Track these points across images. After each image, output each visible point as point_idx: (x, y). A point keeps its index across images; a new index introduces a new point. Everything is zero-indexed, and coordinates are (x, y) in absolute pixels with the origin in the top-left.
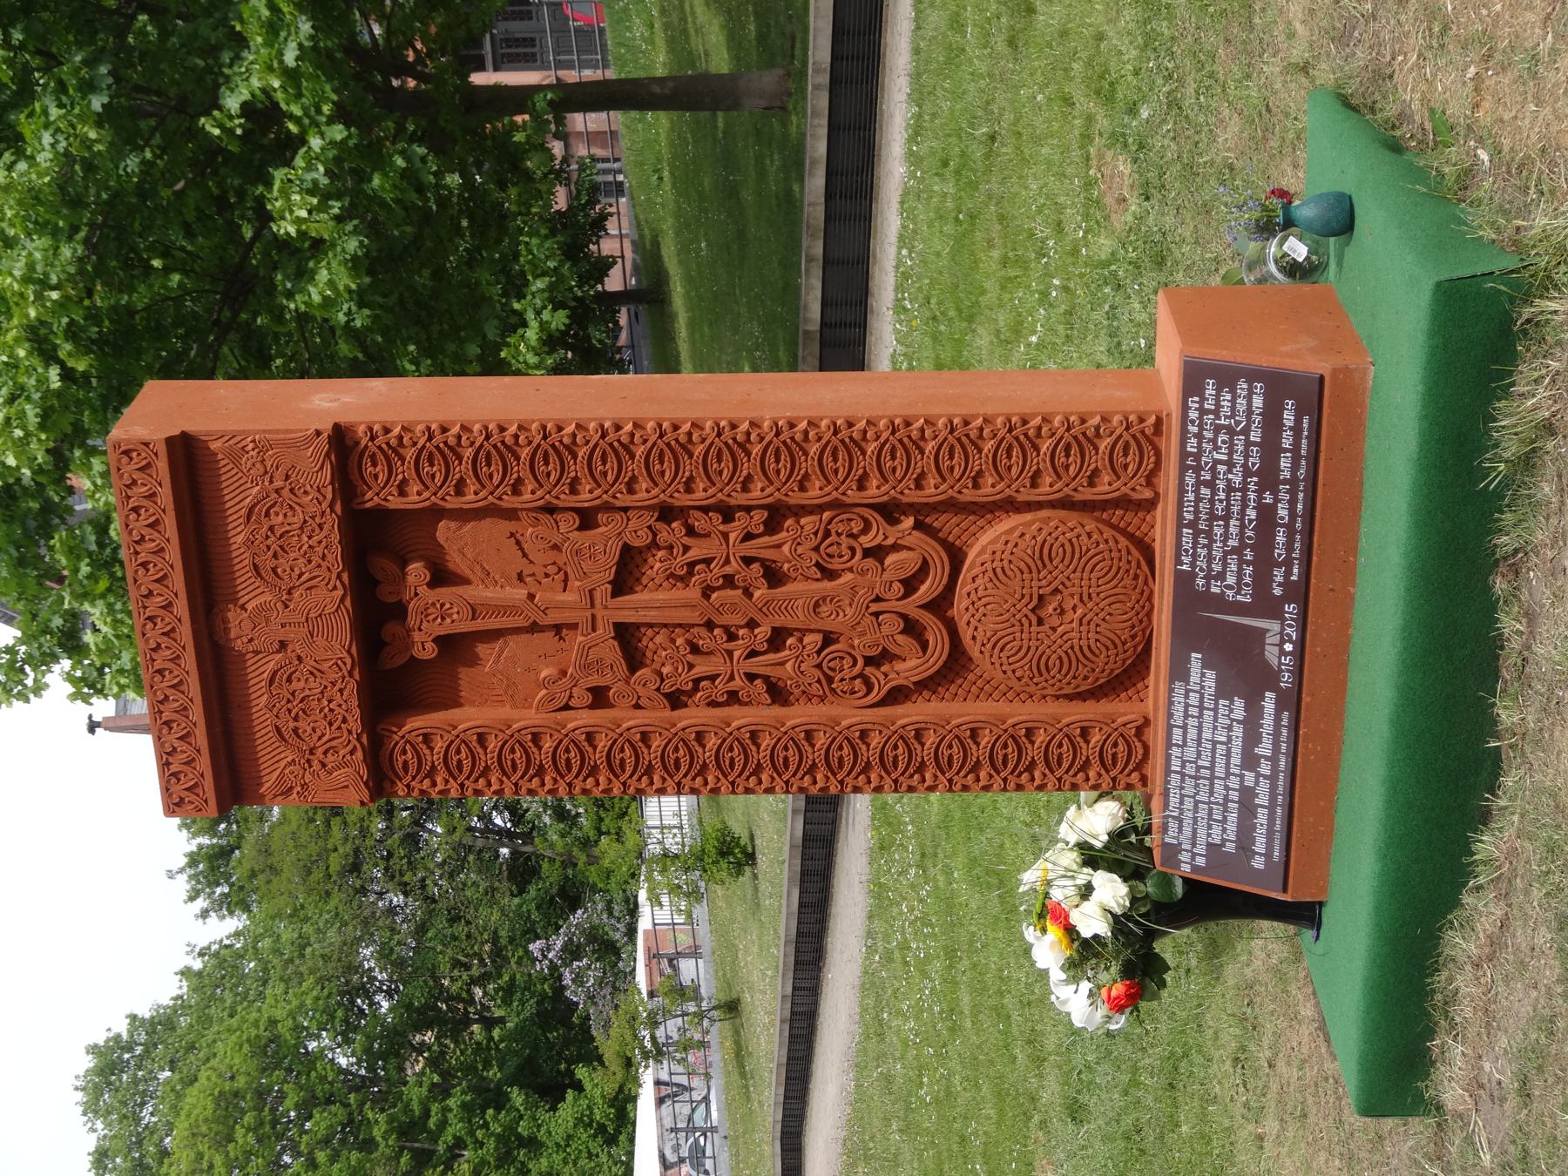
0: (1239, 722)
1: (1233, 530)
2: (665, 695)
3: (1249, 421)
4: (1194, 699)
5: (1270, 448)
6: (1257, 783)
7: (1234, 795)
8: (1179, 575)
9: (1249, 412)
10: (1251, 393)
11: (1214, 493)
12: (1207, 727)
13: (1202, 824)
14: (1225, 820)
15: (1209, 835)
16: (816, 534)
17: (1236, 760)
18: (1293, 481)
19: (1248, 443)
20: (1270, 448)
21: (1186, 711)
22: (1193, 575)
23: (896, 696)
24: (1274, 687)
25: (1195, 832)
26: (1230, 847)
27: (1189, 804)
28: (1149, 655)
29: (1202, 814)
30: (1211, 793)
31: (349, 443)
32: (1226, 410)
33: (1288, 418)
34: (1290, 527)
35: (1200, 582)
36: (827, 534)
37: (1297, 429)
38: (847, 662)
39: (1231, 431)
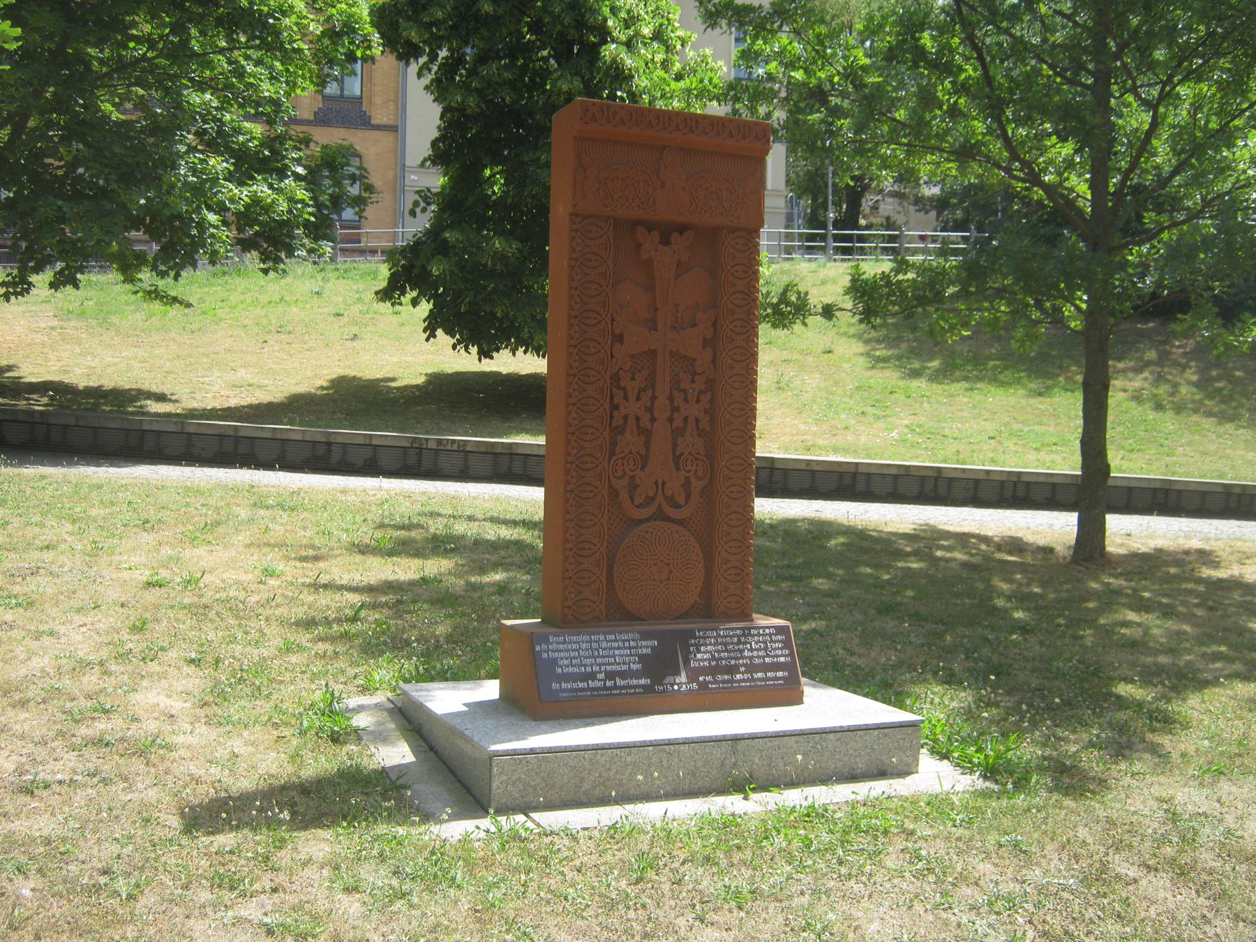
1: (722, 654)
4: (632, 643)
5: (766, 668)
7: (589, 669)
9: (777, 656)
10: (785, 656)
11: (736, 644)
13: (567, 654)
14: (573, 666)
17: (608, 668)
18: (753, 680)
20: (766, 668)
24: (653, 684)
25: (561, 651)
26: (559, 670)
29: (572, 654)
31: (753, 234)
32: (774, 646)
33: (780, 674)
34: (732, 681)
35: (693, 641)
36: (697, 459)
37: (776, 678)
38: (633, 468)
39: (766, 649)
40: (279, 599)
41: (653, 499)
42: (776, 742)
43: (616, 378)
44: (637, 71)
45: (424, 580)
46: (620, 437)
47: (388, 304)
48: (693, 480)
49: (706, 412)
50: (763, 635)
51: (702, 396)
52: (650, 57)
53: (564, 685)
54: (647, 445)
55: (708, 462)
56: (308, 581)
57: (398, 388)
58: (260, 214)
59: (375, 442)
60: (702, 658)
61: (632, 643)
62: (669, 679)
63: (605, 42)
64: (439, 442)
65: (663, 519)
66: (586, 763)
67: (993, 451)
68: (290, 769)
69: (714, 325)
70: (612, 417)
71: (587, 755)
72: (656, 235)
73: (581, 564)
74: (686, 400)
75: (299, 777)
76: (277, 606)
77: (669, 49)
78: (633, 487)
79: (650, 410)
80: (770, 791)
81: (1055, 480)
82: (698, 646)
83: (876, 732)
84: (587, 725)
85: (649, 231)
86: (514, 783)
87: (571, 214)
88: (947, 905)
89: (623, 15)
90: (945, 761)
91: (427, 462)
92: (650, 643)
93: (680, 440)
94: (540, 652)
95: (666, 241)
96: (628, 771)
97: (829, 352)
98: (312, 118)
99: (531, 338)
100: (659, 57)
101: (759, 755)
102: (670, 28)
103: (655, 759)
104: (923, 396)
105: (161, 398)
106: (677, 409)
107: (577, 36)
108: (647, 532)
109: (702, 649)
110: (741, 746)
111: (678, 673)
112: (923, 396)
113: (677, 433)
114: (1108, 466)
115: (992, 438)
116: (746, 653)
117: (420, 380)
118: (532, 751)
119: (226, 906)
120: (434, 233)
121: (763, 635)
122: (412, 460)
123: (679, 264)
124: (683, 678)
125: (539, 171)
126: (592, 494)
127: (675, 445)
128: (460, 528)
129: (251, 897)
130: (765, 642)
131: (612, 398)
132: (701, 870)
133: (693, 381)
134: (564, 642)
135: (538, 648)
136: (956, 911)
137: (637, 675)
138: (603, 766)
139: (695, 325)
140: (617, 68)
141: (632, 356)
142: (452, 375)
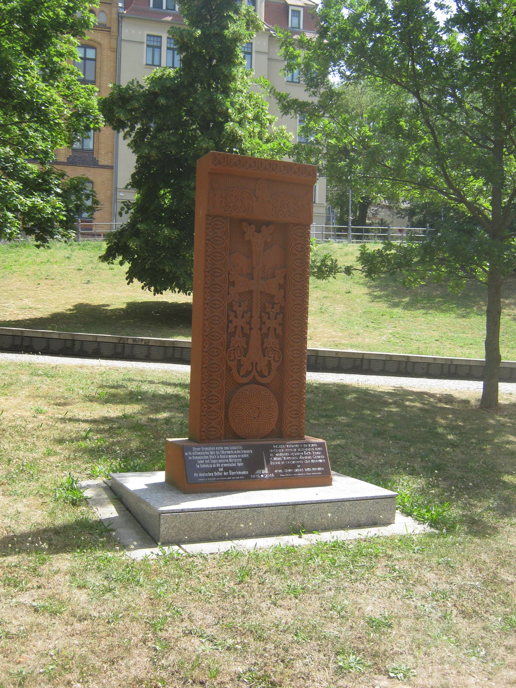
0: (237, 465)
2: (232, 302)
4: (238, 452)
5: (312, 465)
6: (220, 472)
7: (214, 466)
8: (272, 445)
9: (318, 459)
11: (295, 452)
14: (206, 464)
15: (199, 460)
16: (275, 347)
18: (305, 472)
19: (310, 460)
20: (312, 465)
21: (235, 450)
22: (273, 449)
25: (199, 456)
26: (198, 466)
27: (207, 453)
28: (237, 438)
29: (205, 457)
30: (213, 459)
33: (319, 469)
34: (293, 473)
35: (272, 451)
36: (275, 351)
39: (312, 455)
40: (44, 426)
41: (250, 372)
42: (317, 506)
43: (230, 305)
44: (245, 138)
45: (125, 416)
46: (232, 338)
47: (106, 263)
48: (272, 362)
49: (280, 324)
51: (278, 316)
52: (252, 130)
53: (201, 475)
54: (248, 343)
55: (280, 352)
56: (60, 416)
57: (111, 310)
58: (36, 214)
59: (99, 340)
60: (277, 459)
61: (238, 452)
62: (258, 472)
63: (227, 121)
64: (134, 340)
65: (256, 384)
66: (212, 517)
67: (438, 348)
68: (49, 520)
69: (285, 277)
70: (228, 327)
71: (213, 513)
73: (210, 408)
74: (269, 318)
75: (54, 525)
76: (43, 430)
77: (262, 125)
78: (240, 365)
79: (249, 323)
80: (313, 533)
81: (471, 364)
82: (274, 453)
83: (372, 501)
84: (213, 496)
85: (250, 224)
86: (173, 528)
87: (207, 215)
88: (409, 596)
89: (237, 106)
90: (410, 517)
91: (127, 351)
92: (248, 451)
93: (266, 340)
94: (187, 456)
95: (258, 231)
96: (236, 522)
97: (349, 293)
98: (66, 161)
99: (184, 284)
100: (257, 130)
101: (307, 514)
102: (263, 114)
103: (250, 515)
104: (400, 317)
106: (264, 323)
107: (212, 118)
108: (247, 390)
109: (277, 455)
110: (298, 508)
111: (264, 469)
112: (400, 317)
113: (265, 336)
114: (500, 356)
115: (437, 340)
116: (301, 458)
117: (124, 306)
118: (182, 511)
119: (12, 596)
120: (132, 225)
121: (310, 447)
122: (119, 350)
124: (266, 471)
125: (190, 192)
126: (217, 369)
127: (263, 343)
128: (145, 387)
129: (26, 591)
130: (311, 451)
131: (228, 316)
132: (275, 576)
133: (273, 308)
134: (201, 451)
135: (186, 454)
136: (414, 599)
137: (241, 469)
138: (222, 519)
139: (274, 277)
140: (234, 136)
142: (142, 303)
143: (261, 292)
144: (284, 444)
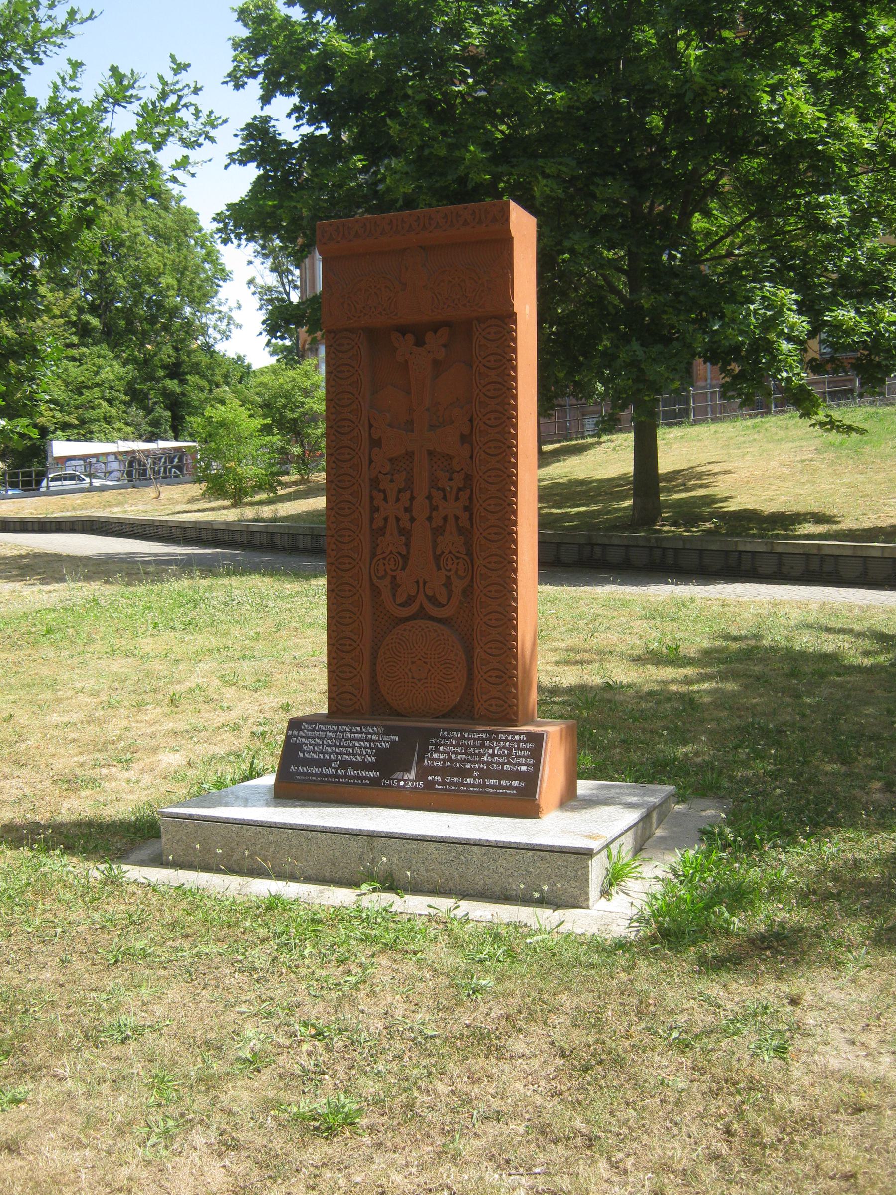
2: (377, 477)
3: (514, 765)
4: (375, 737)
5: (501, 775)
7: (327, 757)
8: (438, 730)
12: (362, 744)
13: (312, 741)
14: (314, 752)
18: (484, 786)
19: (503, 764)
20: (501, 775)
23: (376, 591)
26: (301, 755)
27: (322, 734)
32: (519, 753)
33: (516, 783)
34: (462, 784)
36: (458, 558)
37: (510, 787)
39: (509, 756)
42: (414, 845)
45: (608, 687)
50: (510, 741)
53: (301, 769)
54: (407, 544)
58: (841, 337)
60: (437, 757)
62: (398, 775)
72: (410, 338)
78: (395, 586)
79: (375, 510)
82: (437, 745)
83: (530, 854)
85: (404, 335)
92: (391, 738)
95: (420, 342)
96: (272, 849)
103: (295, 842)
105: (819, 518)
109: (441, 749)
110: (378, 843)
111: (408, 771)
113: (438, 531)
116: (485, 759)
118: (190, 817)
121: (510, 741)
123: (436, 363)
124: (412, 775)
130: (510, 749)
133: (451, 479)
141: (391, 460)
143: (430, 453)
144: (461, 731)
